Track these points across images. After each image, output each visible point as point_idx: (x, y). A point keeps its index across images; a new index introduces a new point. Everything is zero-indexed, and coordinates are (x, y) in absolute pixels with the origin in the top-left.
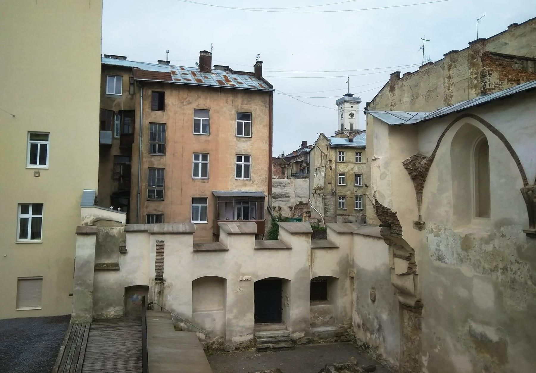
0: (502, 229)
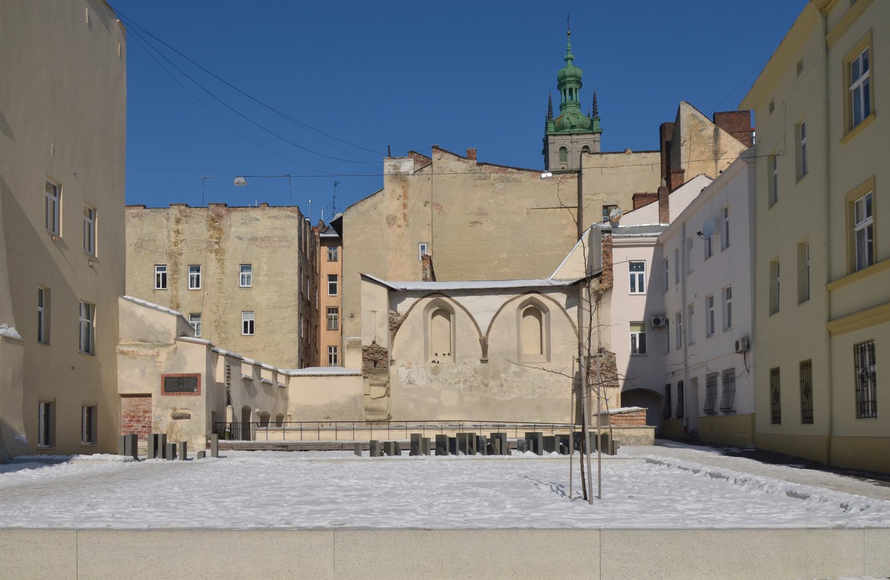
0: (464, 360)
